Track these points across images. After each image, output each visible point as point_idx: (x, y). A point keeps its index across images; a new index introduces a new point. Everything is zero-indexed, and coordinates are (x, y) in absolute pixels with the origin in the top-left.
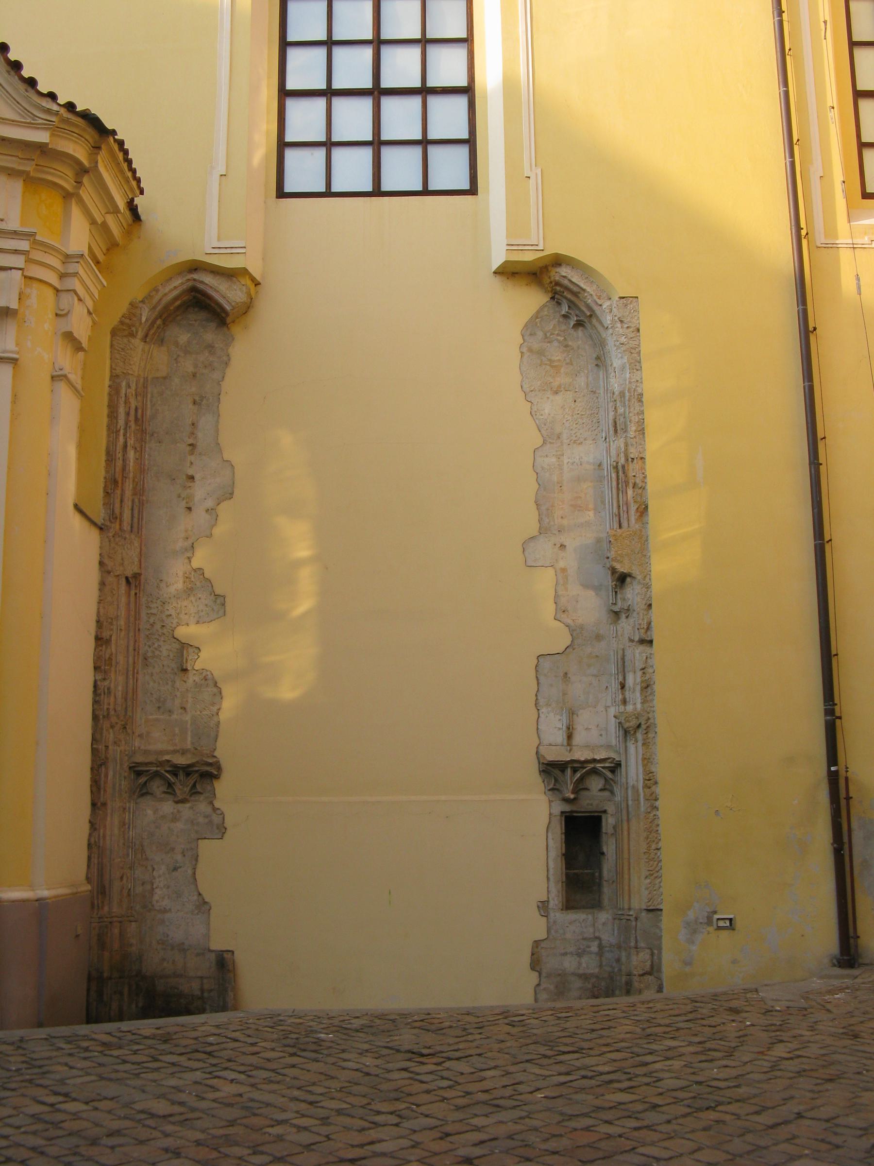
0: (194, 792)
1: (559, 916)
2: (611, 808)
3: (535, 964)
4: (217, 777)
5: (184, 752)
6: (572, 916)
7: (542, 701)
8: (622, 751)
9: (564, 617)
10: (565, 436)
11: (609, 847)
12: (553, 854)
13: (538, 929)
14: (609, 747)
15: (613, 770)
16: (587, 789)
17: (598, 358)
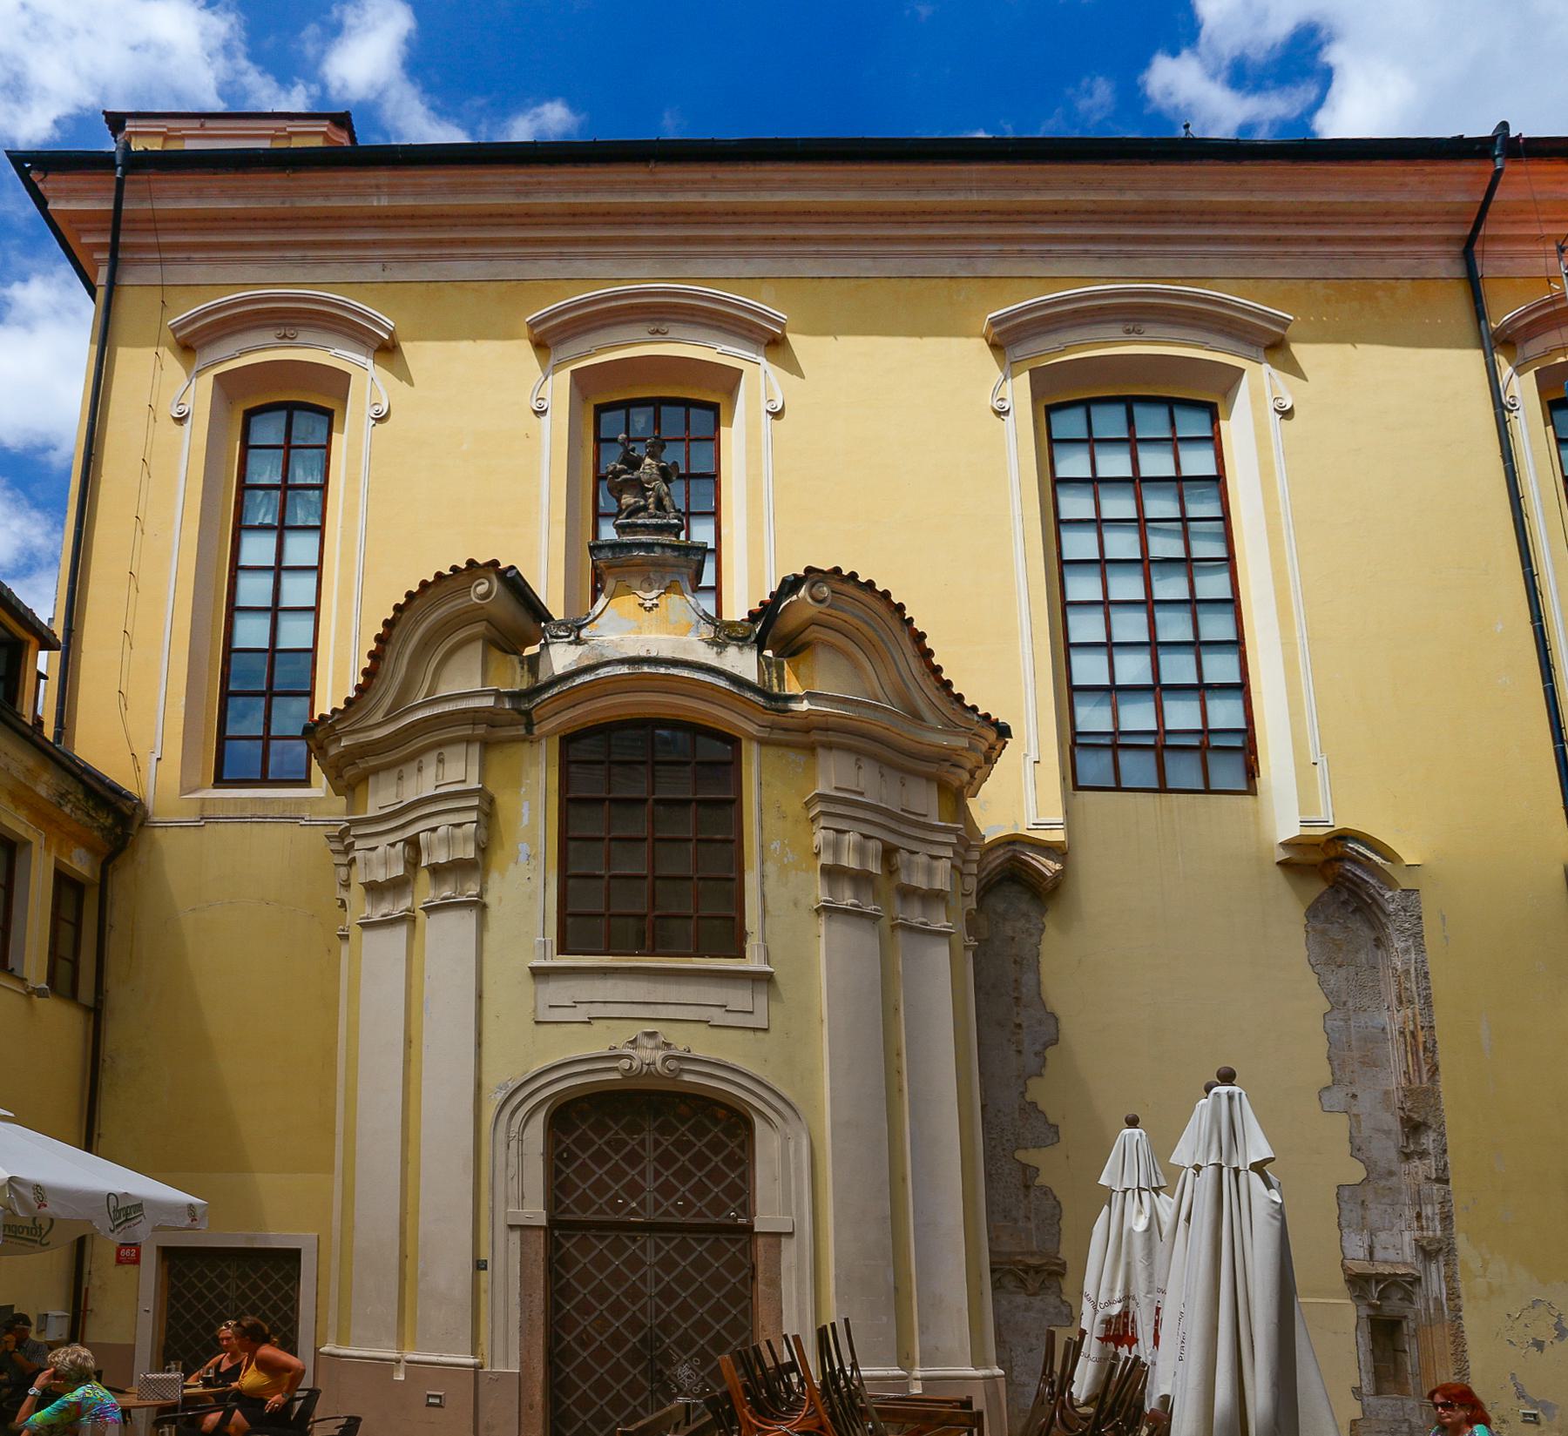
0: (1043, 1287)
1: (1372, 1400)
2: (1411, 1316)
4: (1062, 1275)
5: (1032, 1254)
6: (1380, 1401)
7: (1344, 1223)
8: (1420, 1267)
9: (1359, 1155)
10: (1350, 1004)
11: (1411, 1347)
12: (1362, 1349)
14: (1405, 1264)
17: (1377, 939)
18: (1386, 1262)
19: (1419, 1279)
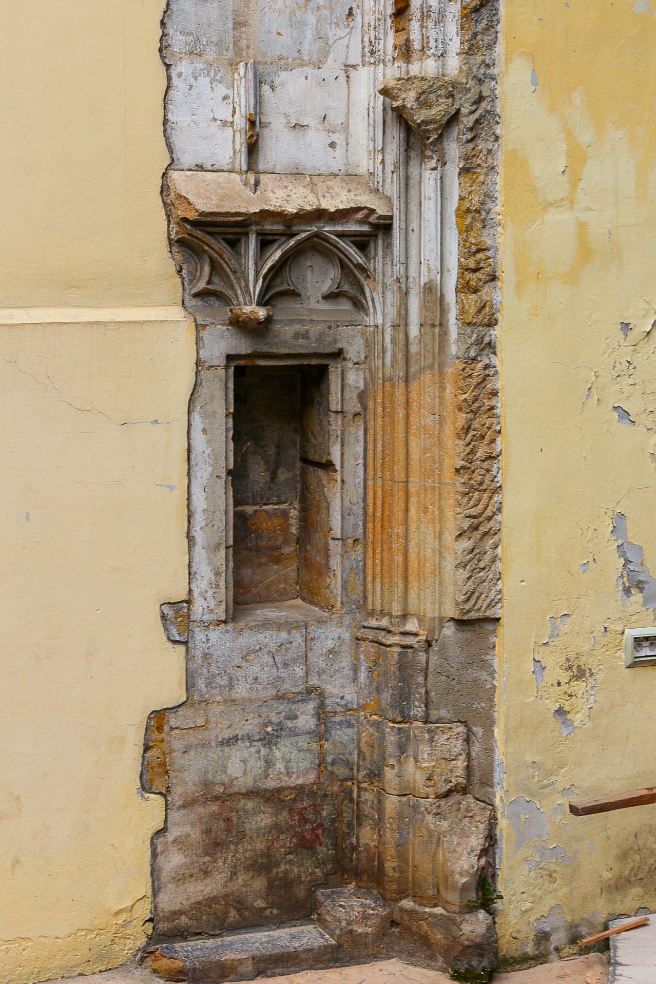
1: (217, 641)
2: (355, 349)
3: (154, 775)
7: (178, 42)
8: (392, 189)
11: (346, 449)
12: (203, 472)
13: (161, 677)
14: (350, 177)
15: (362, 243)
16: (294, 294)
18: (296, 174)
19: (384, 227)
